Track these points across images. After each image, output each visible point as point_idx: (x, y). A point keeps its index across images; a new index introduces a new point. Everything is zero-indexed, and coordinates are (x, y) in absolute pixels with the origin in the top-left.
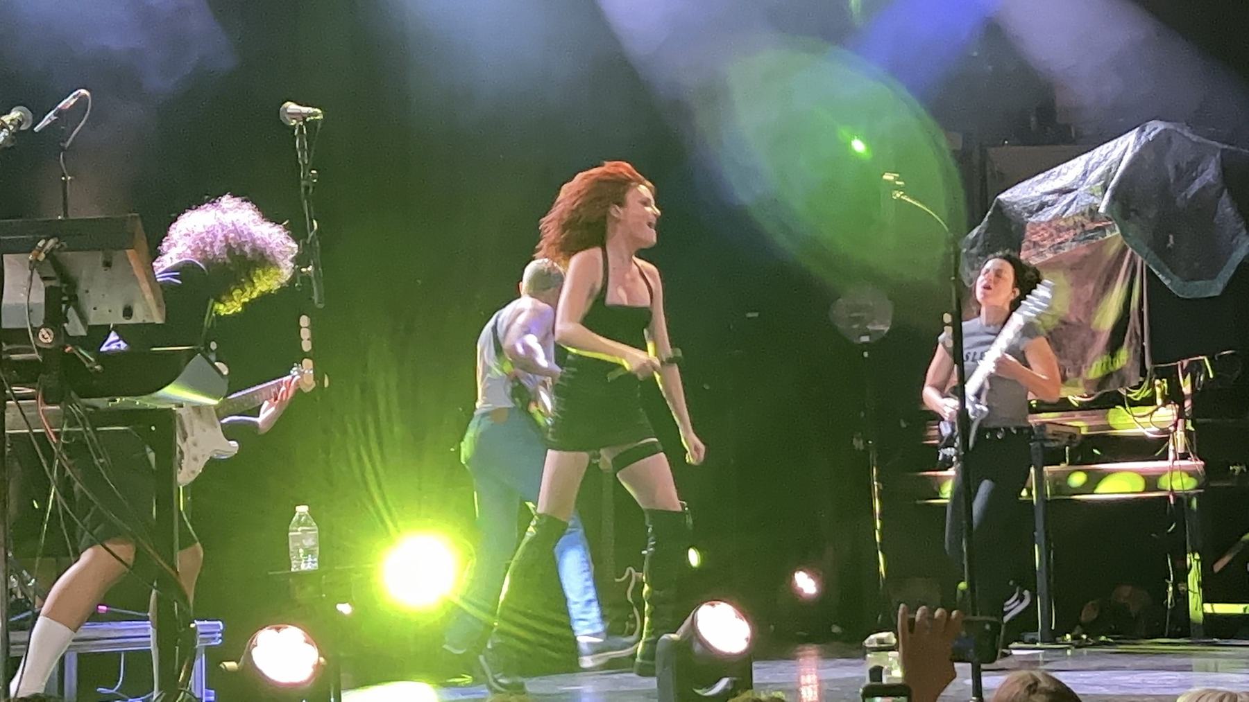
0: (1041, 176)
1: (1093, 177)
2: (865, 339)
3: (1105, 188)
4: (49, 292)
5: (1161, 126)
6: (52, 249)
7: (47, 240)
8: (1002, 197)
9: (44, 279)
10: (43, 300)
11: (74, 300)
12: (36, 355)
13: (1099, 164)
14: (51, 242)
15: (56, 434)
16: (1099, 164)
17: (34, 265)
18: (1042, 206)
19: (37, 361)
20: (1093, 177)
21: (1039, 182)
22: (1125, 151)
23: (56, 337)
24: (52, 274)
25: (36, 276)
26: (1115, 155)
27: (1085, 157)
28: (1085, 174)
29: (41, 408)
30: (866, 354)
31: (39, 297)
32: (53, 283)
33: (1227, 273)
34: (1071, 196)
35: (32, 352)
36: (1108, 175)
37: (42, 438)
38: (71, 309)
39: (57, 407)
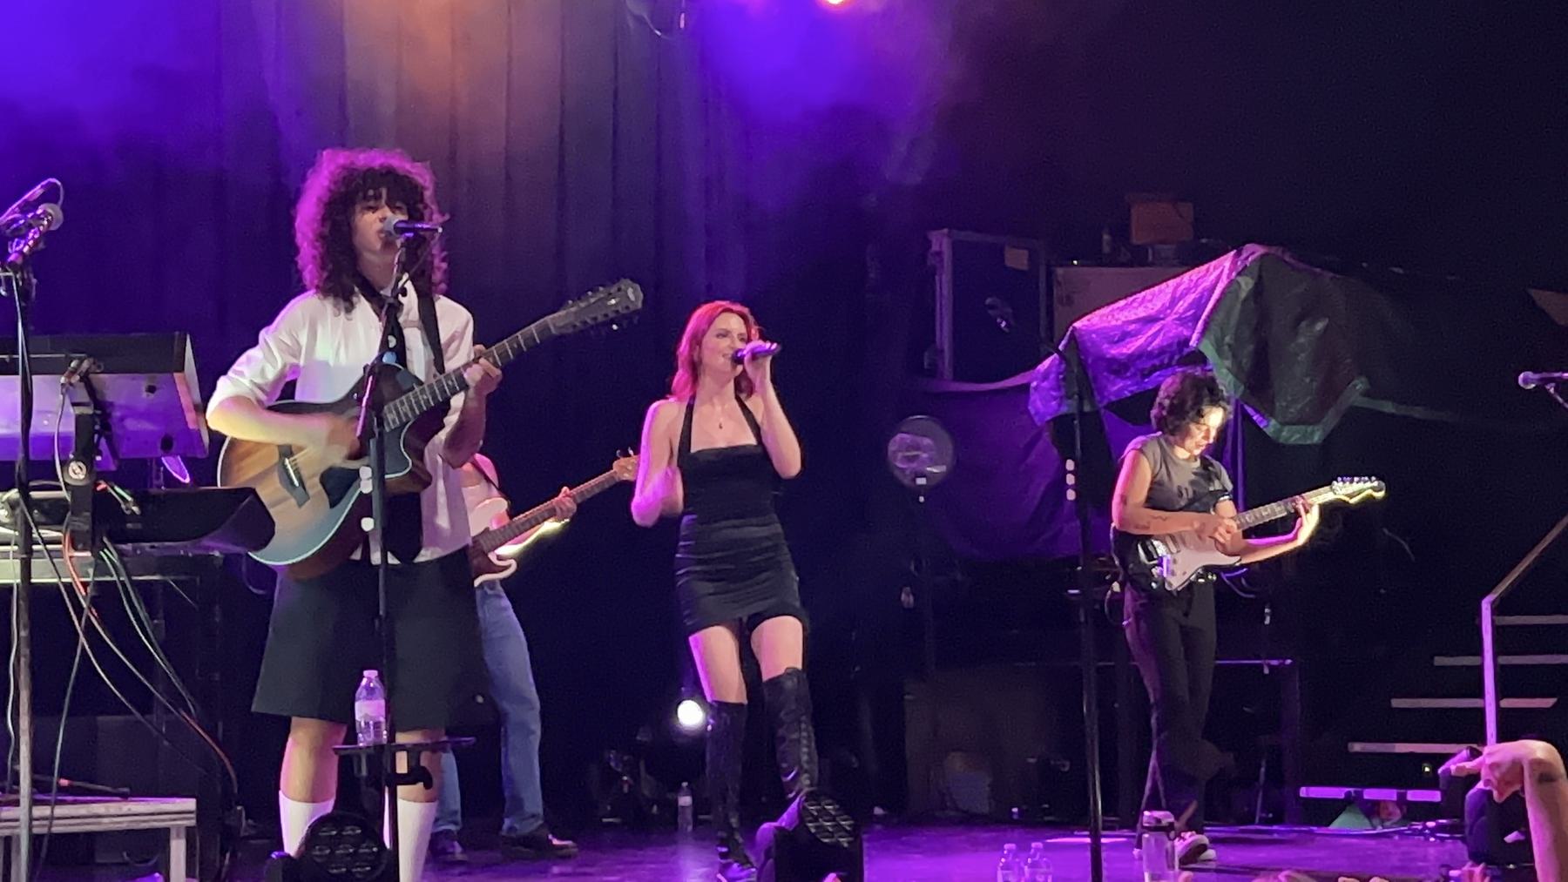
0: (1122, 303)
1: (1182, 306)
2: (921, 481)
3: (1196, 318)
4: (78, 418)
5: (1260, 250)
6: (88, 372)
7: (81, 360)
8: (1077, 324)
9: (74, 404)
10: (72, 429)
11: (106, 427)
12: (63, 494)
13: (1188, 291)
14: (86, 365)
15: (85, 585)
16: (1188, 291)
17: (67, 389)
18: (1125, 336)
19: (64, 500)
20: (1182, 306)
21: (1122, 309)
22: (1219, 278)
23: (89, 471)
24: (85, 398)
25: (68, 402)
26: (1207, 284)
27: (1172, 283)
28: (1174, 301)
29: (67, 555)
30: (922, 499)
31: (70, 428)
32: (89, 411)
33: (1331, 420)
34: (1157, 327)
35: (59, 489)
36: (1199, 305)
37: (69, 587)
38: (103, 440)
39: (88, 554)
